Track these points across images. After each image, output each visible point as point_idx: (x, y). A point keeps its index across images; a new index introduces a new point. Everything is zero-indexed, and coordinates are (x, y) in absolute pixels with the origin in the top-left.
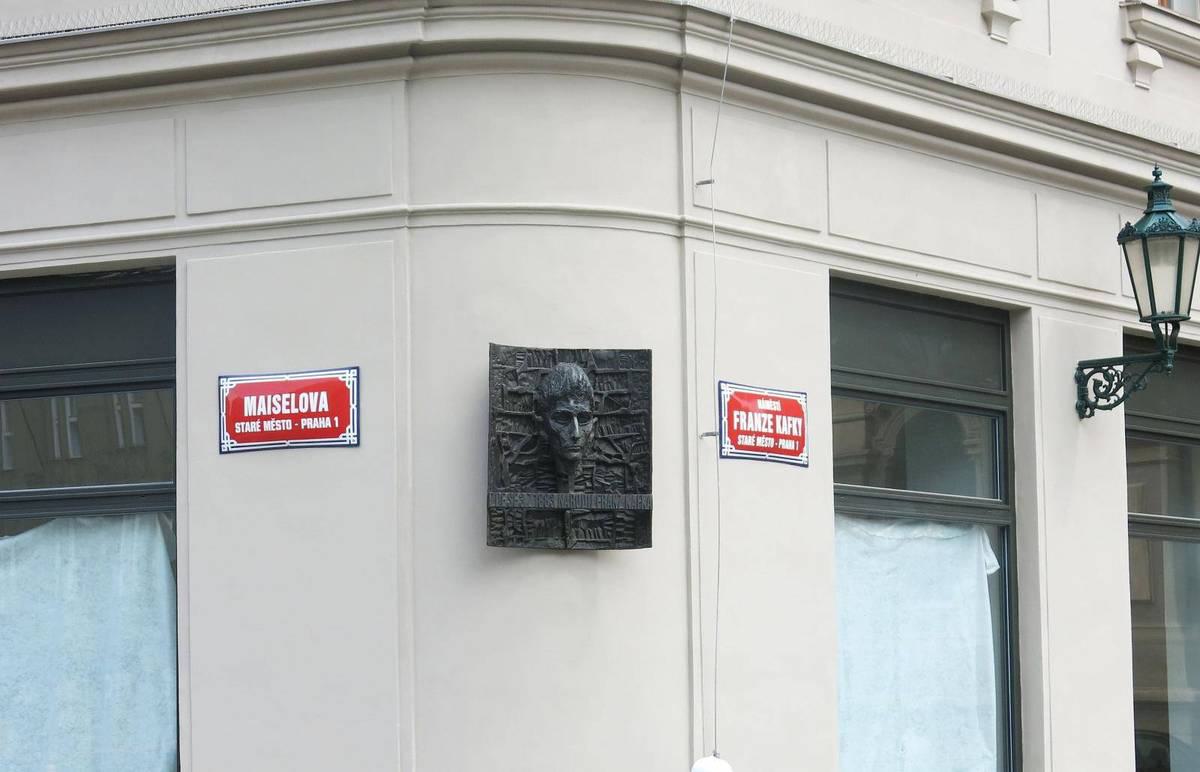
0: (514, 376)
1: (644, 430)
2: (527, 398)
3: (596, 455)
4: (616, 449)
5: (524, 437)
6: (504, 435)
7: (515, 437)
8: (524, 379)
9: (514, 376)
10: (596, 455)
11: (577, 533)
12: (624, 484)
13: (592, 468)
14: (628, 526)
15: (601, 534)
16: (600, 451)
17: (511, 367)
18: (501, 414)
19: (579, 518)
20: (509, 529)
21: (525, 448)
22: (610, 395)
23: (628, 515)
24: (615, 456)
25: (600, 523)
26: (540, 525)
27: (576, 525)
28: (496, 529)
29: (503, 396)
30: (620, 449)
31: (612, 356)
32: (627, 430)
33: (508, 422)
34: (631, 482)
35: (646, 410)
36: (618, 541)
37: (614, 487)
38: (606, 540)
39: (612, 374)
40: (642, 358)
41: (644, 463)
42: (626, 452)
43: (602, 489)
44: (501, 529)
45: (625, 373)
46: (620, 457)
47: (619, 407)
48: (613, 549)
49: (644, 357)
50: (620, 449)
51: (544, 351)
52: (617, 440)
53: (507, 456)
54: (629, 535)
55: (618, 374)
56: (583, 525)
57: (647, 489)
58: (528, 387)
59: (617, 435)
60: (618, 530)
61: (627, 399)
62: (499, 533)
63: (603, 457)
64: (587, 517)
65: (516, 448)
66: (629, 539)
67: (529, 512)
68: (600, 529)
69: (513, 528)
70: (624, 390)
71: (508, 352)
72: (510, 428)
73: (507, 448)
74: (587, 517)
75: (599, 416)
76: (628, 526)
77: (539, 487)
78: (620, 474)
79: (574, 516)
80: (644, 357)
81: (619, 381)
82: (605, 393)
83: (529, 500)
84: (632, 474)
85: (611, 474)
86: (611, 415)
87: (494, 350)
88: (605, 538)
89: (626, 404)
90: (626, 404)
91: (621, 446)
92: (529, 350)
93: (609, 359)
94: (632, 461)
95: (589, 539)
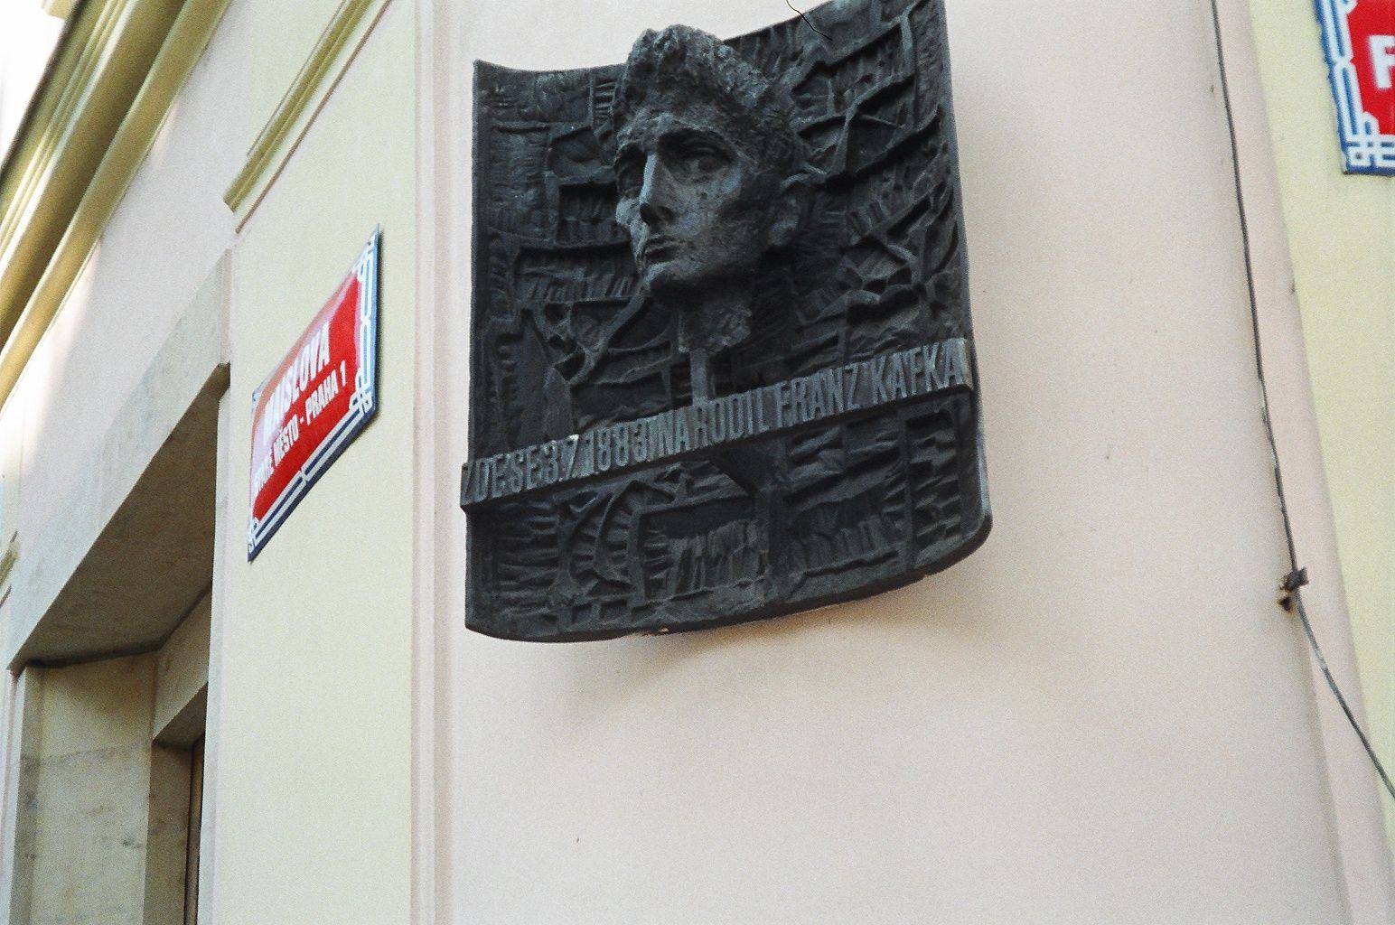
4: (899, 260)
13: (834, 341)
19: (812, 503)
25: (871, 501)
26: (688, 553)
38: (887, 549)
44: (546, 583)
46: (903, 275)
52: (898, 231)
60: (923, 503)
71: (564, 89)
74: (834, 496)
82: (849, 115)
85: (890, 338)
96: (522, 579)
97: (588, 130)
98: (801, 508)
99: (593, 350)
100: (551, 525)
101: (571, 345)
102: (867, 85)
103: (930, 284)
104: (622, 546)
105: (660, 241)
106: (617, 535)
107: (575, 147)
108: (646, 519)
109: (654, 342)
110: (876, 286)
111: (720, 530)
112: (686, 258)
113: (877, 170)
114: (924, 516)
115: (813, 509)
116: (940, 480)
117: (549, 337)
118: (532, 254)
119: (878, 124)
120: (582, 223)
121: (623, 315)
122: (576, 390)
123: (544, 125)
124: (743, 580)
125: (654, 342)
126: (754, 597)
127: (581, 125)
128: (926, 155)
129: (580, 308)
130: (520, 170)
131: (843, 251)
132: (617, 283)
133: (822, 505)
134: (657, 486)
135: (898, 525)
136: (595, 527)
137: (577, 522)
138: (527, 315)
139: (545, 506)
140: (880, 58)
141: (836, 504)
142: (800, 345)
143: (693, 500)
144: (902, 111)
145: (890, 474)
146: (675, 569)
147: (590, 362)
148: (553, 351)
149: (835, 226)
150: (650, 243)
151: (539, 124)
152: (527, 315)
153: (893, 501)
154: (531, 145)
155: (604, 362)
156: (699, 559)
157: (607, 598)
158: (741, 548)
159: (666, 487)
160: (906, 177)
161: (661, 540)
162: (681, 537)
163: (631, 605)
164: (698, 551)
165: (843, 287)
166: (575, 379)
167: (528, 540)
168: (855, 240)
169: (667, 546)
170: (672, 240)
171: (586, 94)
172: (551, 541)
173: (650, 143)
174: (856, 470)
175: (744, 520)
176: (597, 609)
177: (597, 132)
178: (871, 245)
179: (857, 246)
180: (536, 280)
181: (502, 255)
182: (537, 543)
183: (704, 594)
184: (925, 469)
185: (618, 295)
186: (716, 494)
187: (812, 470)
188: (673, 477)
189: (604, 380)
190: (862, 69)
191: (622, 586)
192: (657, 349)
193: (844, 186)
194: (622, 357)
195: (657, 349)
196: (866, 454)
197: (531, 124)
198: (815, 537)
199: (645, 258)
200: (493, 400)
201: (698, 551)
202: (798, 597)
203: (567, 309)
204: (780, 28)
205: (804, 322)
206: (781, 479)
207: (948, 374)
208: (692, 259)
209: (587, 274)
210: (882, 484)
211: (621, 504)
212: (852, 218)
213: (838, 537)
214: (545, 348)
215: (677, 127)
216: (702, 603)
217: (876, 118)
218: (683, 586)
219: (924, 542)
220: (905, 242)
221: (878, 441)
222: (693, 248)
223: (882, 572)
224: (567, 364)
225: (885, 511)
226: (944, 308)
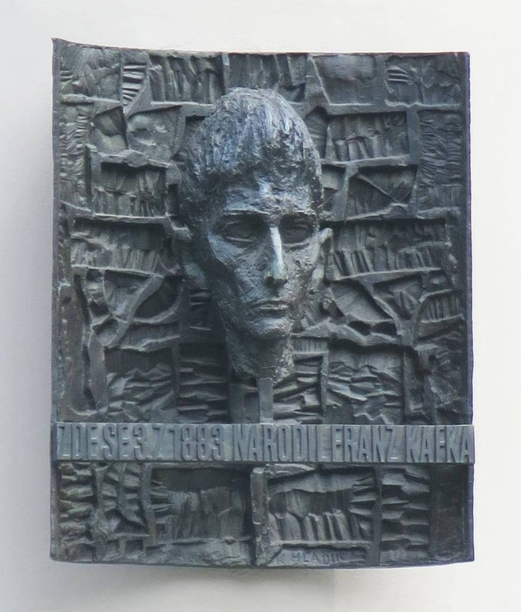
0: (118, 122)
1: (452, 258)
2: (149, 182)
3: (329, 326)
5: (142, 279)
6: (92, 276)
7: (121, 281)
8: (142, 132)
9: (118, 122)
10: (329, 326)
11: (281, 523)
12: (402, 398)
13: (319, 359)
14: (412, 506)
15: (342, 527)
16: (338, 315)
17: (110, 102)
18: (84, 223)
19: (287, 488)
20: (109, 515)
21: (143, 310)
22: (366, 170)
23: (410, 478)
24: (381, 328)
25: (341, 500)
27: (279, 507)
28: (73, 517)
29: (88, 174)
30: (390, 310)
31: (367, 69)
32: (408, 261)
33: (102, 241)
34: (420, 393)
35: (456, 210)
36: (386, 546)
37: (376, 405)
38: (355, 543)
39: (368, 117)
40: (442, 73)
41: (451, 345)
42: (404, 315)
43: (346, 412)
44: (85, 516)
45: (402, 114)
46: (389, 328)
47: (385, 201)
48: (376, 564)
49: (450, 72)
50: (390, 310)
51: (194, 59)
52: (383, 286)
53: (100, 330)
54: (413, 530)
55: (382, 116)
56: (297, 505)
57: (459, 412)
58: (152, 151)
59: (383, 274)
60: (387, 516)
61: (406, 180)
63: (345, 331)
64: (308, 486)
65: (123, 307)
66: (417, 540)
67: (158, 473)
68: (339, 515)
69: (116, 513)
70: (401, 159)
71: (102, 64)
72: (106, 258)
73: (101, 309)
74: (308, 486)
75: (338, 227)
76: (412, 506)
77: (184, 407)
78: (391, 374)
79: (274, 482)
80: (450, 72)
81: (386, 135)
83: (158, 440)
84: (420, 373)
86: (366, 224)
88: (353, 537)
89: (404, 194)
90: (404, 194)
91: (392, 302)
92: (156, 58)
93: (361, 78)
94: (422, 340)
95: (311, 542)
96: (71, 511)
101: (101, 309)
111: (210, 490)
114: (391, 527)
115: (289, 492)
117: (90, 300)
121: (142, 290)
133: (295, 490)
140: (378, 126)
145: (358, 483)
161: (161, 491)
163: (146, 545)
165: (323, 313)
190: (363, 131)
198: (288, 516)
204: (282, 57)
207: (465, 452)
210: (350, 490)
213: (307, 519)
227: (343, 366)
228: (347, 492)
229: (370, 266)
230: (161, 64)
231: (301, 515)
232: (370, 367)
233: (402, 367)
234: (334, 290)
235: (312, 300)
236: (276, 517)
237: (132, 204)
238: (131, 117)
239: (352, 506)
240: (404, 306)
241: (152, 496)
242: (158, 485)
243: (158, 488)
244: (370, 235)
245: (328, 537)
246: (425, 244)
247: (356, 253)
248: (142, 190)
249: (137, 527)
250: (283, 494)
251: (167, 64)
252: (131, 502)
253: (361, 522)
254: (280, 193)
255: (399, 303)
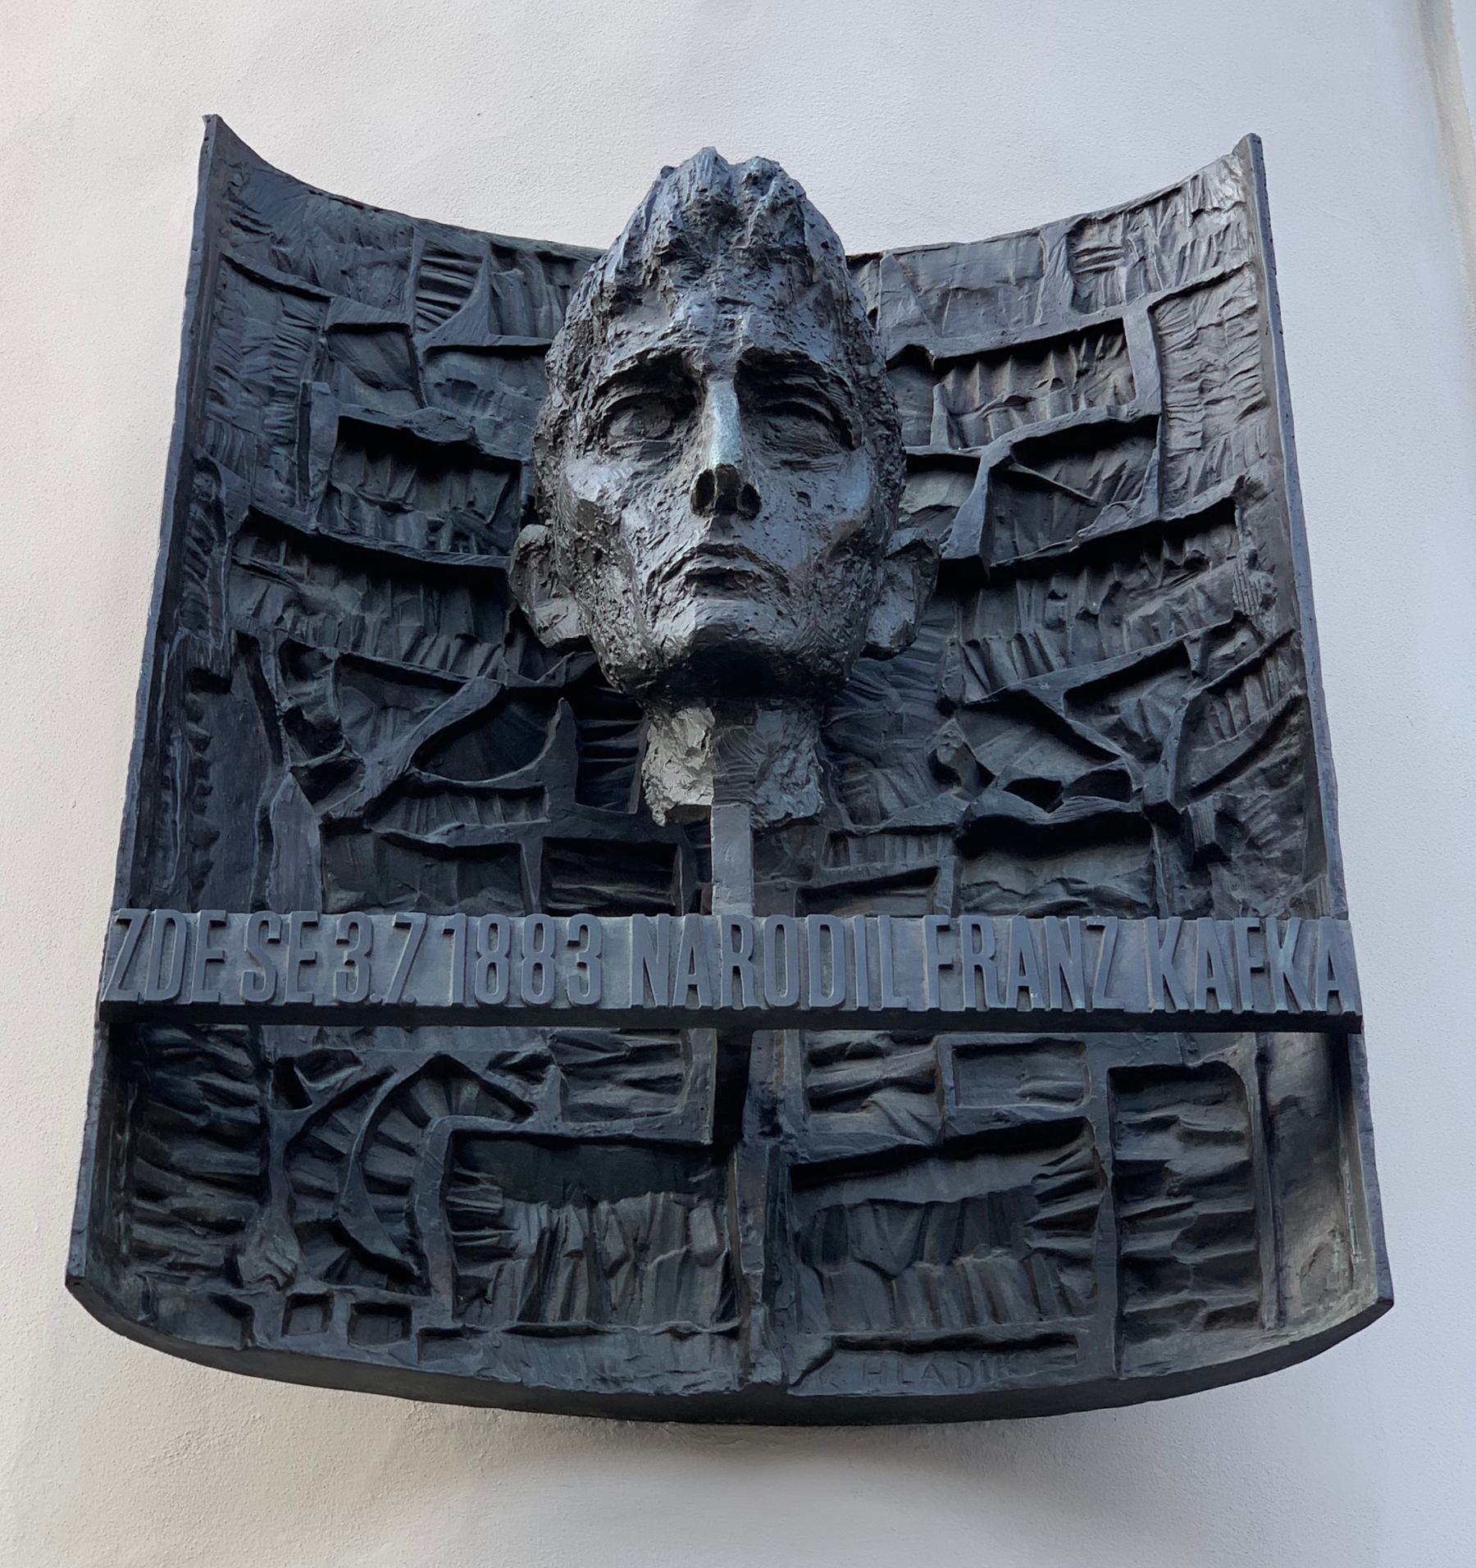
8: (462, 389)
13: (925, 878)
19: (852, 1194)
22: (1035, 451)
24: (1084, 786)
30: (1115, 748)
44: (228, 1228)
45: (1115, 328)
56: (878, 1238)
59: (1091, 673)
62: (209, 1250)
63: (995, 801)
71: (362, 239)
74: (911, 1187)
82: (990, 454)
87: (260, 237)
91: (1118, 730)
92: (505, 252)
96: (177, 1203)
97: (401, 329)
98: (828, 1198)
99: (386, 753)
100: (245, 1102)
101: (324, 735)
102: (1015, 414)
103: (1205, 810)
104: (400, 1188)
105: (728, 553)
106: (390, 1165)
107: (366, 353)
108: (461, 1140)
109: (508, 779)
110: (1042, 791)
111: (624, 1204)
112: (770, 607)
113: (1039, 571)
114: (1144, 1273)
115: (856, 1206)
116: (1189, 1205)
117: (286, 705)
118: (264, 529)
119: (1049, 488)
120: (364, 506)
122: (332, 829)
123: (316, 290)
124: (683, 1323)
125: (508, 779)
126: (709, 1370)
127: (389, 317)
128: (1170, 567)
129: (354, 668)
130: (261, 360)
131: (946, 707)
132: (427, 642)
133: (873, 1202)
134: (496, 1079)
135: (1072, 1280)
136: (341, 1131)
137: (311, 1109)
138: (247, 645)
139: (240, 1057)
141: (908, 1206)
142: (830, 874)
143: (568, 1128)
144: (1117, 476)
146: (519, 1267)
147: (371, 783)
148: (288, 742)
149: (934, 657)
150: (703, 550)
151: (306, 286)
152: (247, 645)
153: (1050, 1226)
154: (285, 319)
155: (400, 791)
156: (576, 1254)
157: (365, 1293)
158: (676, 1252)
159: (511, 1084)
160: (1108, 601)
162: (533, 1200)
164: (574, 1239)
165: (942, 775)
166: (340, 805)
167: (201, 1122)
168: (975, 694)
169: (502, 1211)
170: (752, 557)
171: (403, 266)
172: (252, 1137)
173: (717, 357)
174: (957, 1149)
175: (683, 1198)
176: (341, 1311)
177: (421, 342)
178: (1017, 709)
179: (975, 707)
180: (261, 584)
181: (215, 509)
182: (214, 1134)
183: (589, 1332)
184: (1138, 1179)
185: (432, 664)
186: (624, 1126)
187: (851, 1129)
188: (531, 1069)
189: (382, 829)
191: (397, 1275)
192: (511, 797)
193: (960, 584)
194: (437, 790)
195: (511, 797)
196: (1000, 1117)
197: (292, 280)
199: (679, 579)
200: (167, 797)
201: (574, 1239)
202: (814, 1387)
203: (325, 660)
205: (849, 826)
206: (788, 1128)
208: (780, 613)
209: (366, 604)
211: (401, 1099)
212: (969, 651)
214: (272, 727)
215: (780, 346)
216: (573, 1351)
217: (1049, 476)
218: (533, 1308)
219: (1132, 1328)
220: (1112, 719)
221: (1023, 1096)
222: (786, 591)
223: (1028, 1372)
224: (314, 772)
225: (1035, 1245)
226: (1225, 861)
227: (995, 891)
228: (1017, 1193)
229: (1055, 660)
230: (521, 267)
231: (890, 1267)
232: (1062, 881)
233: (1151, 869)
234: (968, 730)
235: (910, 750)
236: (820, 1275)
237: (432, 538)
238: (435, 353)
239: (1035, 1234)
240: (1147, 732)
241: (453, 1204)
242: (473, 1181)
243: (472, 1189)
244: (1054, 596)
245: (972, 1317)
246: (1192, 584)
247: (1020, 638)
248: (463, 508)
249: (397, 1275)
250: (837, 1213)
251: (538, 270)
252: (384, 1214)
253: (1061, 1270)
254: (740, 309)
255: (1136, 726)
